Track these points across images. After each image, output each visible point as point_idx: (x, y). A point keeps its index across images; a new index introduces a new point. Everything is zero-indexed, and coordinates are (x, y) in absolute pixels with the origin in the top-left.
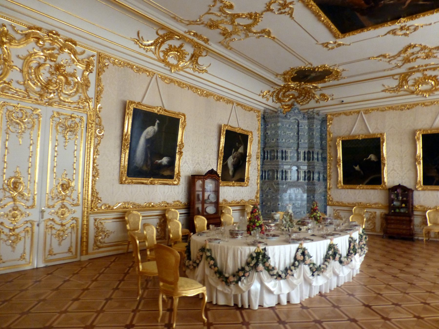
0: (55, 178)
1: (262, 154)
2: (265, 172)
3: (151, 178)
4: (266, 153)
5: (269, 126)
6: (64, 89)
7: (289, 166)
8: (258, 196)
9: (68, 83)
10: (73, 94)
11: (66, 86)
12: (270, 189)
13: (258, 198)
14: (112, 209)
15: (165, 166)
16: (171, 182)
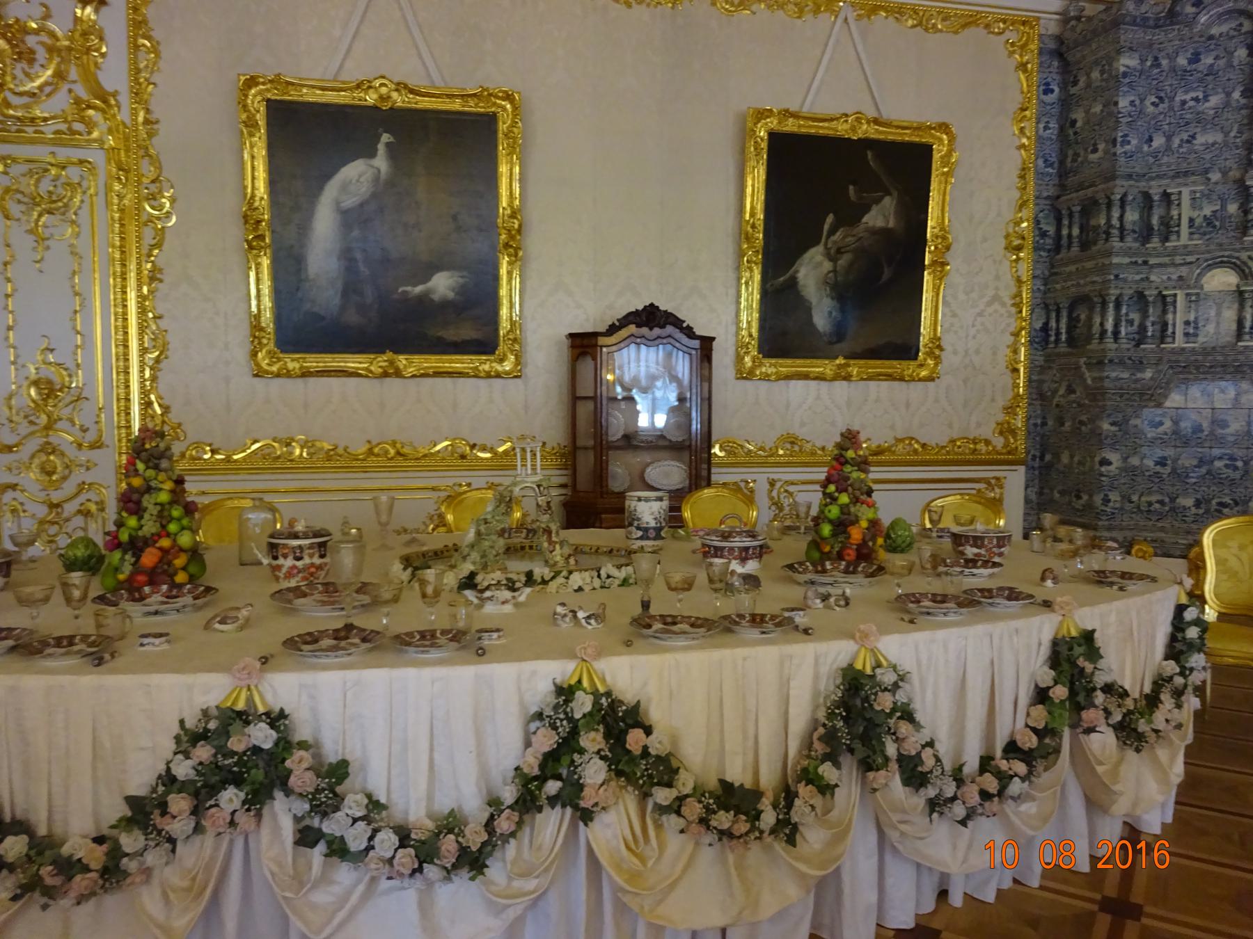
0: (13, 363)
1: (1051, 230)
2: (1058, 311)
3: (383, 352)
4: (1066, 222)
5: (1081, 84)
6: (14, 78)
7: (1184, 271)
8: (1019, 422)
9: (27, 56)
10: (48, 89)
11: (19, 66)
12: (1070, 391)
13: (1013, 432)
14: (228, 460)
15: (444, 305)
16: (486, 367)
